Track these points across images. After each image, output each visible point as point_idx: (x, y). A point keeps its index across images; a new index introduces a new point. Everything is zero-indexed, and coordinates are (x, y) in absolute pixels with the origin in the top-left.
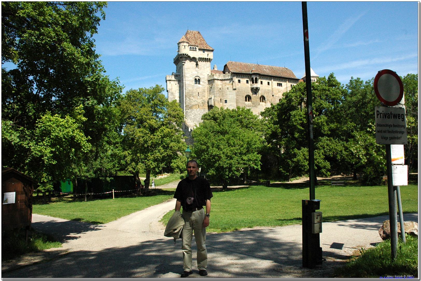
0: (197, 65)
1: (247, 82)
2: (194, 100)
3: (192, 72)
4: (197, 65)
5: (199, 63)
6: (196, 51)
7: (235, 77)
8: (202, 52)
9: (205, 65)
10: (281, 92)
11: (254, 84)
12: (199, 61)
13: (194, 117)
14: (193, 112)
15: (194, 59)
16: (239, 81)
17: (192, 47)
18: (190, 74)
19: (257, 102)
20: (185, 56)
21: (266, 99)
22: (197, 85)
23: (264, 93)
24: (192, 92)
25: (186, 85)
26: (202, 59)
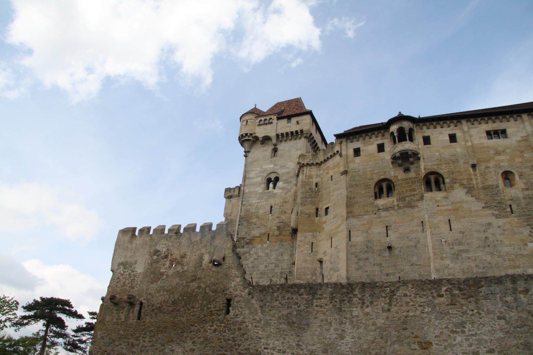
0: (275, 150)
2: (258, 224)
3: (261, 167)
4: (275, 150)
5: (281, 147)
6: (271, 123)
8: (284, 122)
9: (292, 146)
12: (281, 141)
13: (252, 262)
14: (252, 252)
15: (267, 139)
17: (263, 119)
18: (257, 172)
19: (415, 193)
20: (247, 138)
21: (447, 181)
23: (438, 164)
26: (282, 137)
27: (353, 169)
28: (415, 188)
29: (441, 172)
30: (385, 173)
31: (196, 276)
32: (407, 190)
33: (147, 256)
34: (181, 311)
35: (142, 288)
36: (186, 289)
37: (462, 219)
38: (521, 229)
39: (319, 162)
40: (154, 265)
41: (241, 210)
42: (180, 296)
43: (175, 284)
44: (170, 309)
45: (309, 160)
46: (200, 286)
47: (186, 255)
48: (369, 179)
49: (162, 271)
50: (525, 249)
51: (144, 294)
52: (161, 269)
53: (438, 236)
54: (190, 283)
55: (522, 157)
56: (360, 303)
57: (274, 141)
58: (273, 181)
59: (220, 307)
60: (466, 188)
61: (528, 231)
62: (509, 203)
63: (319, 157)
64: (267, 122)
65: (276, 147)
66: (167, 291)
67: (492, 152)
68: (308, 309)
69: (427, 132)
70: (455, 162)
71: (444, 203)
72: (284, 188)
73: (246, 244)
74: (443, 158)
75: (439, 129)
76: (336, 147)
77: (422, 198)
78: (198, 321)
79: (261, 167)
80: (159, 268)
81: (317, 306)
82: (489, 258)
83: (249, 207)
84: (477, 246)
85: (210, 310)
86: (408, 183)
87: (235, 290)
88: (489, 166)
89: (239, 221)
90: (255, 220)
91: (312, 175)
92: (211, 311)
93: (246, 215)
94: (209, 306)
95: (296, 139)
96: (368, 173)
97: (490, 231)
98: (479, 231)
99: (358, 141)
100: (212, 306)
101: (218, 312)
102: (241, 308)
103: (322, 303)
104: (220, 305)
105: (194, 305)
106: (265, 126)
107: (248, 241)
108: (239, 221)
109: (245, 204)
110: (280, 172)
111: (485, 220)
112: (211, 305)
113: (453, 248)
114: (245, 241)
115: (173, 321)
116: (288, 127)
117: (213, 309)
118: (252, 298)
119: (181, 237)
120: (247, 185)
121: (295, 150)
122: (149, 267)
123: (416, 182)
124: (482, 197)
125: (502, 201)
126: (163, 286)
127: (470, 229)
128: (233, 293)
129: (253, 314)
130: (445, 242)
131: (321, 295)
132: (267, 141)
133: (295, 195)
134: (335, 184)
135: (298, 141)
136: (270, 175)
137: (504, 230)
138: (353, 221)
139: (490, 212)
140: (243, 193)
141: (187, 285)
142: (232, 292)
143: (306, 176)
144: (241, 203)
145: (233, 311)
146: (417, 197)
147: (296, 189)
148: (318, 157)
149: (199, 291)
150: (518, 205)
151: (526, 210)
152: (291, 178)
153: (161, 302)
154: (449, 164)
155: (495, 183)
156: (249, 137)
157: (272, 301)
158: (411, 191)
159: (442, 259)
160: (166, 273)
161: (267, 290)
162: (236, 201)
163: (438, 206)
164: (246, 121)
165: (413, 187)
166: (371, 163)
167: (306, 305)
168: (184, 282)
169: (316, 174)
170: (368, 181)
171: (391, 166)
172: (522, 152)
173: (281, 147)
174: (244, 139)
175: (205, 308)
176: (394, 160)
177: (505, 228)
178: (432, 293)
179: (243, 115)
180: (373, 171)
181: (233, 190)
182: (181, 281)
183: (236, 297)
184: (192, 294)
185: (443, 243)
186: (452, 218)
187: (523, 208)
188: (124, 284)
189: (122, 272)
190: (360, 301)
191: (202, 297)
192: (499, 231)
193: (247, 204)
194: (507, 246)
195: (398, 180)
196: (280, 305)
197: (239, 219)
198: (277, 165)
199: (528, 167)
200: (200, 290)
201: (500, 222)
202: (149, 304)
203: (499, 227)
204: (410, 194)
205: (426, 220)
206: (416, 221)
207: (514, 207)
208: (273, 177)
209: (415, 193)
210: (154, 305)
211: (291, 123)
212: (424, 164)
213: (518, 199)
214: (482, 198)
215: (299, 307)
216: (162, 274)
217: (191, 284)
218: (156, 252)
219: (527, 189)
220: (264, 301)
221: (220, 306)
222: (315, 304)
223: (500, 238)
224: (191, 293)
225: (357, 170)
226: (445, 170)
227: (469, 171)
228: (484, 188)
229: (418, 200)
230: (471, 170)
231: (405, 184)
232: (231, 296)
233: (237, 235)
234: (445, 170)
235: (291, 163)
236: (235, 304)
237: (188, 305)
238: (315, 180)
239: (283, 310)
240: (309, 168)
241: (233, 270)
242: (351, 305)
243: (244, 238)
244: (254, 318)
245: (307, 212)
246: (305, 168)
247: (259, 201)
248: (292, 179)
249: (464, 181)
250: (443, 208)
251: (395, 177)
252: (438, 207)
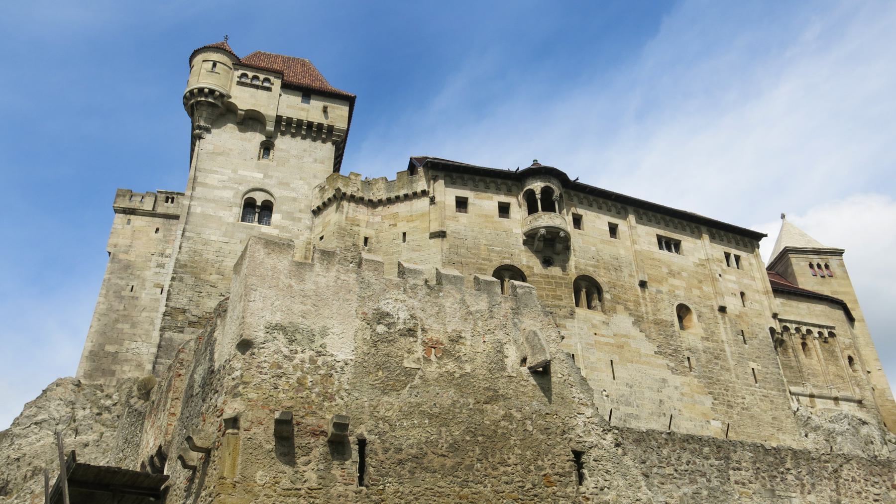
0: (267, 147)
1: (504, 210)
3: (235, 171)
4: (267, 147)
5: (283, 143)
6: (269, 89)
7: (441, 182)
9: (305, 151)
10: (679, 273)
11: (536, 215)
16: (462, 204)
17: (251, 74)
18: (225, 178)
19: (562, 303)
21: (607, 296)
23: (594, 266)
24: (218, 252)
25: (191, 219)
27: (455, 232)
28: (561, 296)
29: (600, 280)
30: (512, 255)
31: (496, 391)
32: (548, 296)
33: (358, 321)
34: (478, 471)
35: (358, 402)
36: (478, 417)
37: (628, 364)
39: (375, 200)
40: (384, 348)
41: (180, 248)
42: (468, 431)
43: (450, 402)
44: (449, 462)
45: (355, 189)
46: (511, 414)
47: (461, 337)
48: (483, 259)
49: (406, 364)
50: (708, 429)
51: (365, 417)
52: (405, 361)
53: (597, 383)
54: (485, 405)
55: (700, 288)
56: (798, 485)
57: (270, 128)
58: (258, 206)
59: (563, 468)
60: (632, 316)
61: (711, 403)
62: (687, 353)
63: (375, 190)
64: (249, 81)
65: (272, 140)
66: (431, 417)
68: (725, 487)
70: (618, 269)
71: (603, 332)
72: (284, 227)
73: (190, 324)
74: (601, 258)
76: (420, 183)
77: (572, 314)
78: (520, 497)
79: (235, 171)
80: (397, 356)
81: (736, 483)
83: (199, 247)
84: (650, 412)
85: (543, 473)
86: (549, 283)
87: (586, 433)
88: (661, 289)
89: (174, 270)
90: (214, 278)
91: (359, 220)
92: (545, 475)
93: (192, 262)
94: (540, 463)
95: (314, 140)
96: (482, 247)
97: (666, 391)
100: (547, 464)
101: (562, 479)
102: (607, 472)
103: (743, 477)
104: (562, 462)
105: (506, 457)
106: (252, 90)
107: (195, 319)
108: (175, 272)
109: (189, 238)
110: (278, 193)
112: (543, 460)
113: (619, 410)
114: (187, 318)
115: (461, 493)
116: (303, 109)
117: (549, 471)
118: (625, 454)
119: (441, 294)
120: (198, 198)
121: (311, 160)
122: (368, 349)
123: (562, 286)
124: (654, 335)
125: (679, 349)
126: (419, 405)
127: (640, 383)
128: (585, 439)
129: (633, 488)
130: (607, 396)
131: (739, 462)
132: (251, 122)
133: (306, 248)
134: (414, 251)
135: (319, 143)
136: (257, 193)
137: (682, 394)
139: (666, 361)
140: (188, 213)
141: (478, 410)
142: (581, 437)
143: (346, 217)
144: (181, 232)
145: (593, 479)
146: (563, 312)
147: (309, 237)
148: (372, 189)
149: (510, 427)
151: (707, 370)
152: (300, 211)
153: (418, 444)
154: (609, 270)
155: (669, 319)
156: (215, 99)
157: (661, 465)
158: (555, 297)
160: (420, 373)
161: (648, 441)
162: (144, 224)
163: (595, 334)
164: (212, 62)
165: (558, 293)
166: (488, 232)
167: (720, 479)
168: (471, 401)
169: (366, 220)
170: (483, 262)
171: (523, 247)
172: (700, 282)
173: (283, 143)
174: (203, 99)
175: (532, 468)
176: (530, 240)
177: (683, 391)
178: (884, 481)
179: (205, 47)
180: (490, 246)
181: (140, 199)
182: (462, 396)
183: (591, 448)
184: (495, 432)
185: (605, 398)
186: (616, 359)
187: (703, 366)
188: (300, 383)
189: (286, 351)
190: (797, 482)
191: (521, 440)
192: (676, 395)
193: (196, 239)
194: (687, 420)
195: (534, 274)
196: (676, 475)
197: (175, 267)
198: (272, 177)
199: (707, 306)
200: (512, 424)
202: (387, 445)
203: (676, 388)
204: (553, 303)
205: (580, 353)
207: (693, 360)
208: (260, 198)
209: (562, 303)
210: (401, 450)
211: (309, 103)
212: (576, 259)
214: (654, 338)
215: (709, 481)
216: (409, 373)
217: (489, 406)
218: (381, 316)
220: (647, 463)
221: (563, 465)
222: (732, 479)
223: (678, 405)
224: (493, 427)
225: (463, 237)
226: (604, 279)
227: (636, 290)
229: (565, 317)
230: (639, 289)
231: (545, 284)
232: (580, 445)
233: (167, 301)
234: (604, 279)
235: (302, 182)
236: (593, 463)
237: (489, 456)
238: (364, 232)
239: (682, 485)
240: (353, 205)
241: (573, 390)
242: (787, 487)
243: (184, 311)
244: (638, 498)
246: (345, 203)
247: (226, 240)
248: (303, 215)
249: (630, 304)
250: (602, 339)
251: (528, 267)
252: (596, 336)
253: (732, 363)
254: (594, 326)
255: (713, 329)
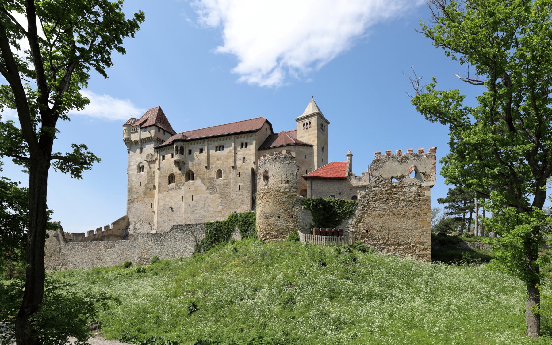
10: (220, 158)
12: (144, 143)
22: (141, 173)
29: (193, 170)
38: (218, 200)
55: (227, 161)
67: (216, 159)
69: (191, 147)
71: (192, 187)
75: (196, 145)
82: (204, 213)
98: (202, 201)
99: (164, 150)
111: (205, 196)
138: (160, 194)
150: (220, 188)
155: (213, 176)
159: (187, 213)
172: (228, 159)
186: (194, 194)
201: (211, 196)
206: (181, 196)
208: (141, 165)
213: (220, 185)
219: (225, 180)
223: (210, 204)
228: (209, 179)
245: (150, 187)
250: (191, 189)
253: (232, 185)
254: (189, 186)
255: (228, 175)
